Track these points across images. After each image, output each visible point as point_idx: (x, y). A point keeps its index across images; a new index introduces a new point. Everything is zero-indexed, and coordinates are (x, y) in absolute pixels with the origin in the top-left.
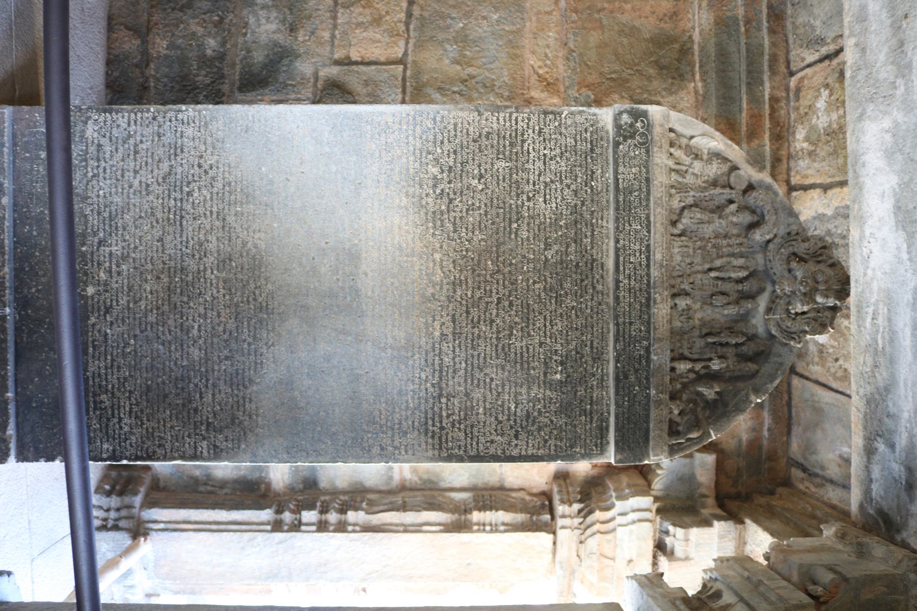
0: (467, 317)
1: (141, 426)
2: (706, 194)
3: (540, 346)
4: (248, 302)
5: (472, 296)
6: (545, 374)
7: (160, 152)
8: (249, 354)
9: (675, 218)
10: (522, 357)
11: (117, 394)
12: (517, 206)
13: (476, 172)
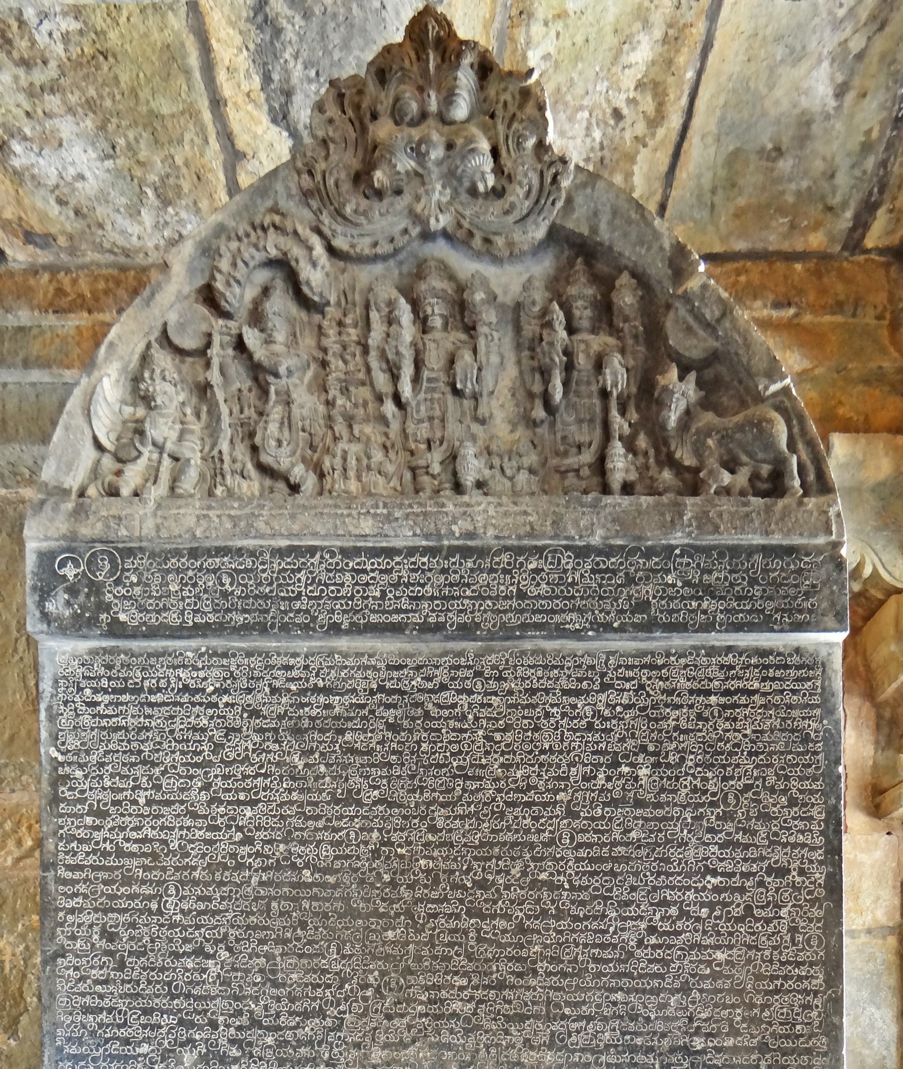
0: (512, 987)
3: (576, 816)
5: (465, 974)
6: (639, 804)
10: (600, 860)
12: (264, 870)
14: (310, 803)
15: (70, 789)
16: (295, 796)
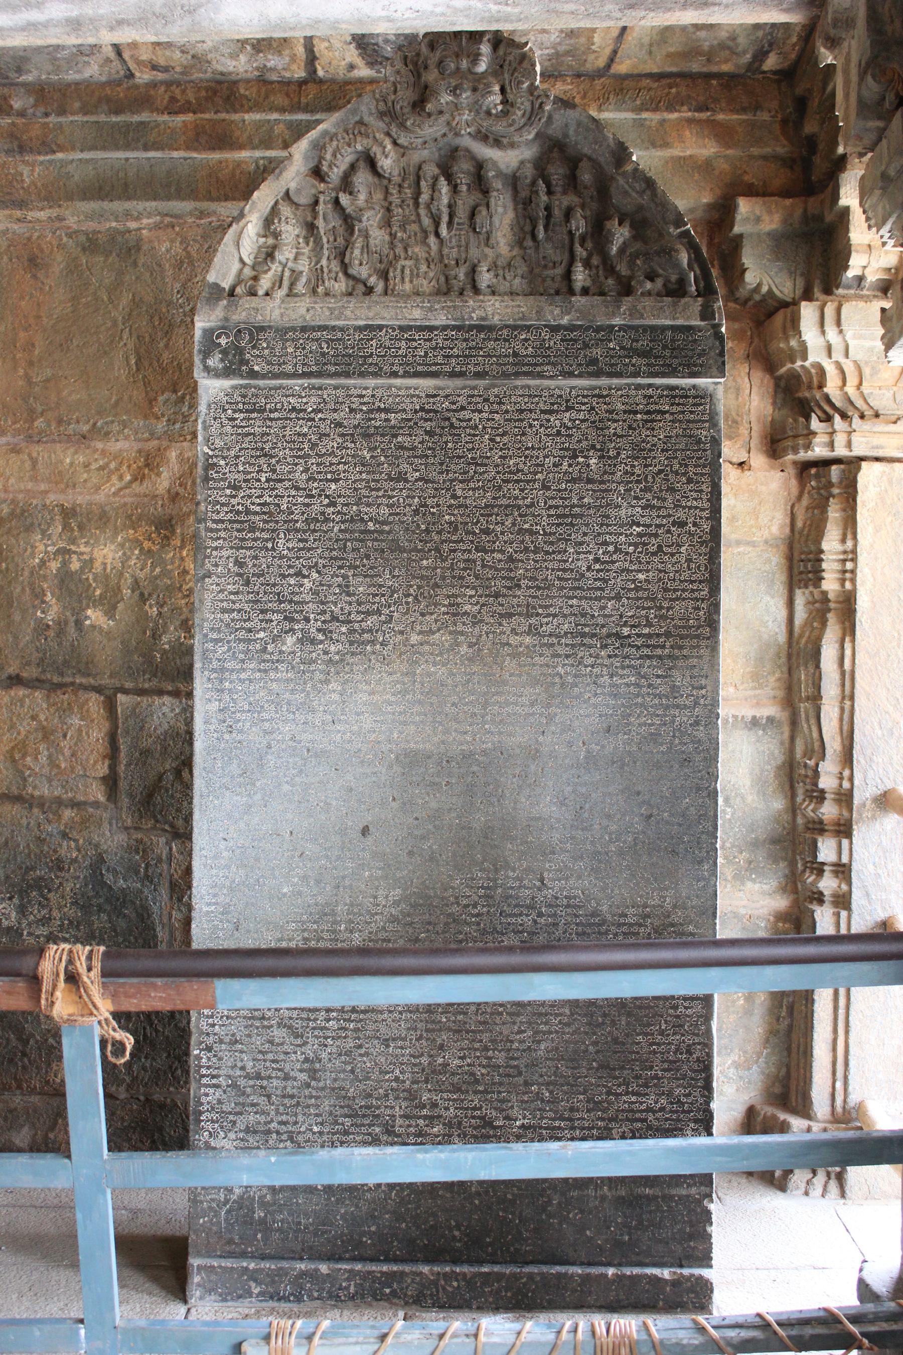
0: (504, 596)
1: (659, 1079)
2: (325, 240)
3: (548, 488)
4: (478, 915)
5: (474, 588)
6: (590, 481)
7: (258, 1041)
8: (555, 915)
9: (361, 288)
10: (565, 516)
11: (611, 1113)
12: (343, 522)
13: (292, 581)
14: (373, 481)
15: (217, 472)
16: (364, 476)
